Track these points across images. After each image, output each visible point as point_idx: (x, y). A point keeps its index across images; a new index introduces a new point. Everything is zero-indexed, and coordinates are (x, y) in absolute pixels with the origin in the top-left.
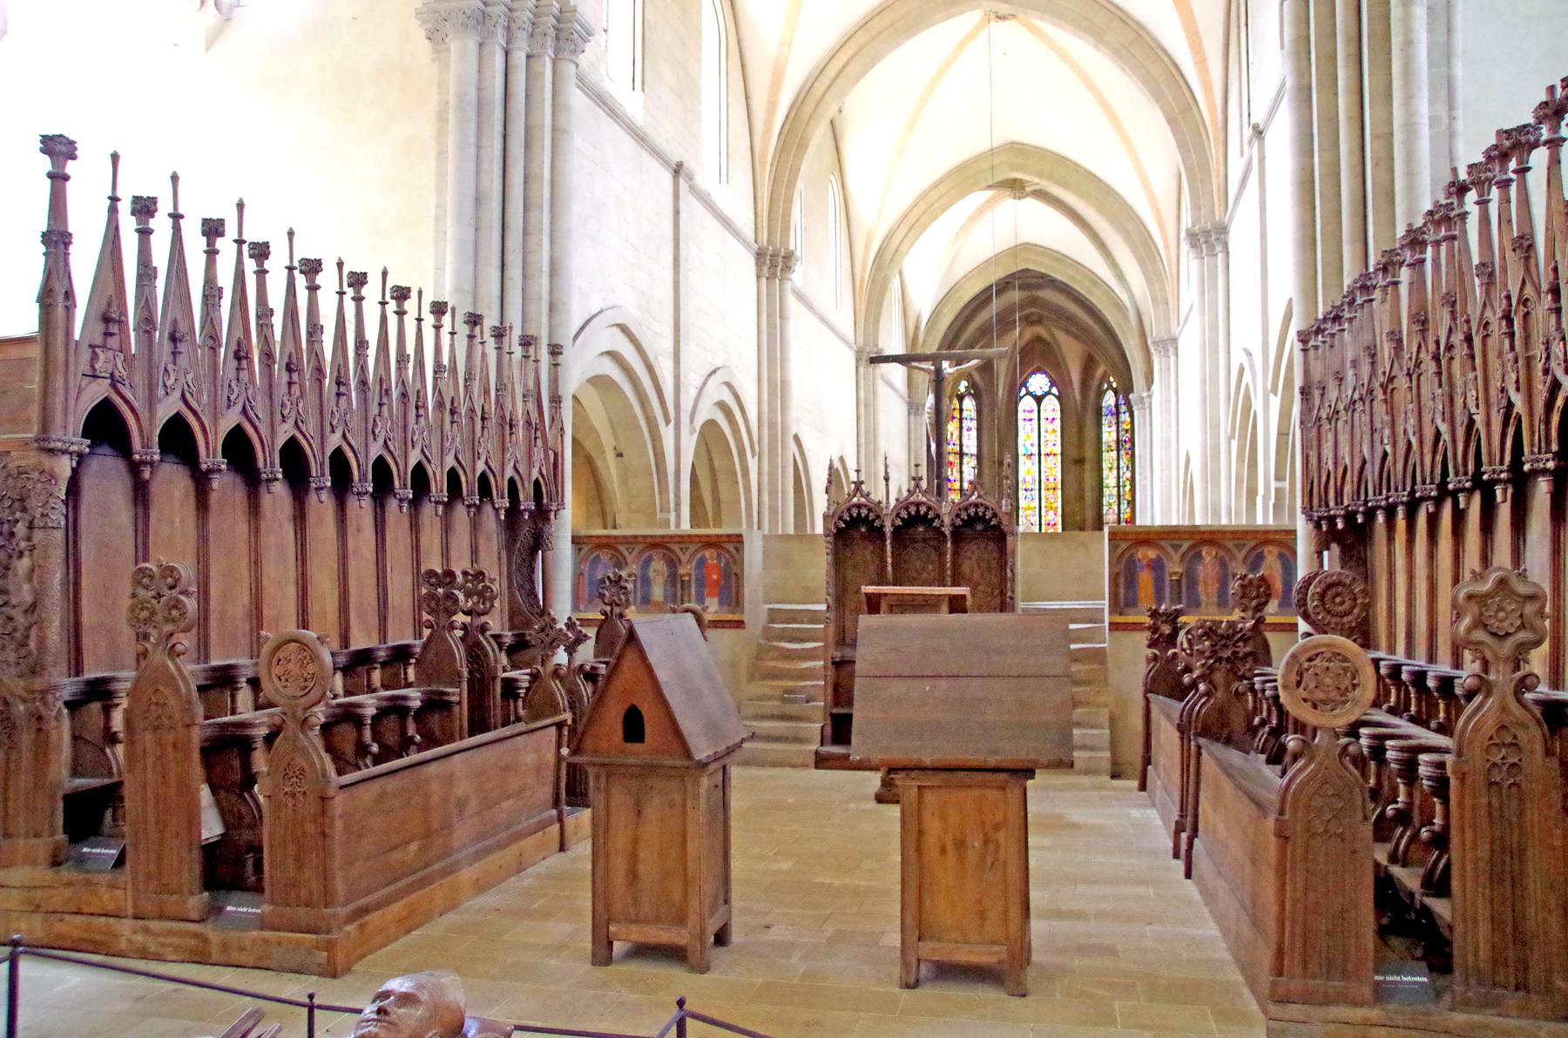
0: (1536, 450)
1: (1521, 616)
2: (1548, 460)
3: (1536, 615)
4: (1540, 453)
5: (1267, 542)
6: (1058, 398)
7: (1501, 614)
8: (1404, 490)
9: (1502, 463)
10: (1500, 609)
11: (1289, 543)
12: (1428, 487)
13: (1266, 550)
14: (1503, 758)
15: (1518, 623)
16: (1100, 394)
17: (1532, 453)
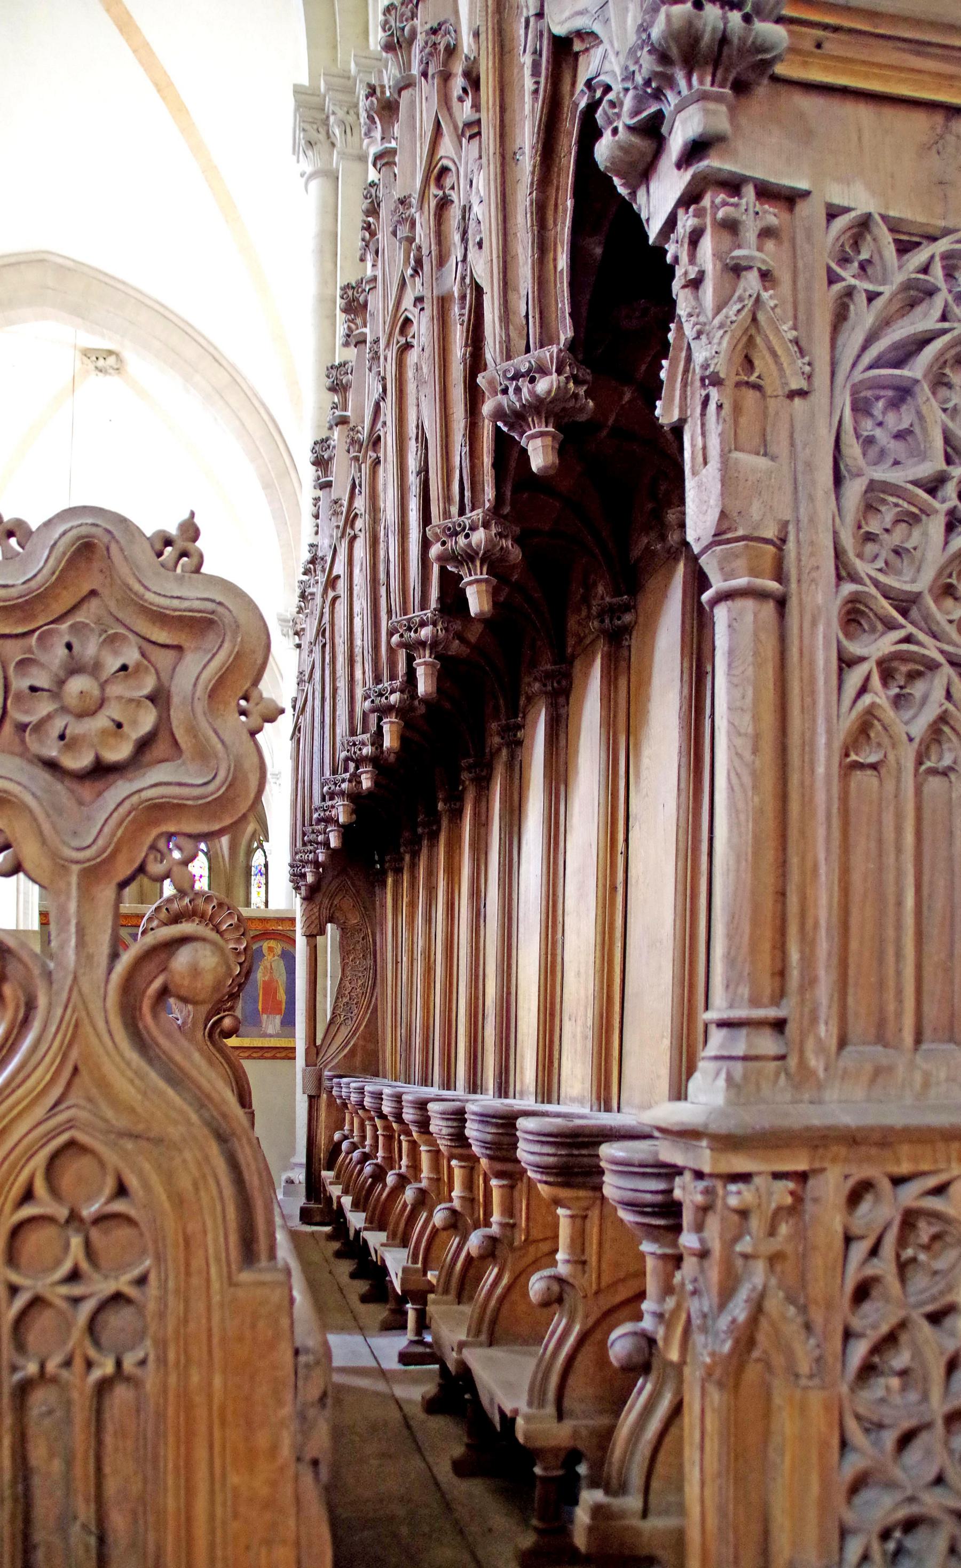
0: (454, 510)
1: (159, 698)
2: (473, 528)
3: (216, 691)
4: (462, 512)
5: (266, 935)
6: (206, 854)
7: (77, 685)
8: (346, 770)
9: (424, 605)
10: (74, 668)
11: (289, 934)
12: (360, 737)
13: (265, 945)
14: (74, 1276)
15: (147, 720)
16: (250, 853)
17: (447, 514)
